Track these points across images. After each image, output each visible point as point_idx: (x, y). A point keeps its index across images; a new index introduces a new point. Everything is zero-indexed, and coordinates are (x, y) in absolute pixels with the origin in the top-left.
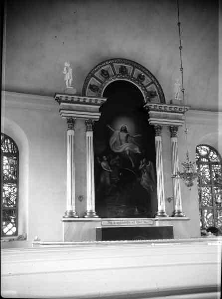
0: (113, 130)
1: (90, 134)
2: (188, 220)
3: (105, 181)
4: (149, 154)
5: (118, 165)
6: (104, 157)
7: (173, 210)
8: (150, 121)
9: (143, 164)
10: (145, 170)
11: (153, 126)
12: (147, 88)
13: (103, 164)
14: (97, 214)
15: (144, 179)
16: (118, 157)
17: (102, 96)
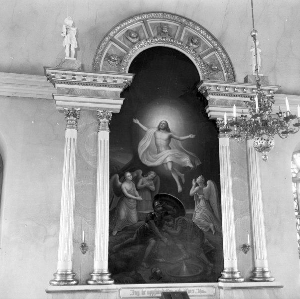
0: (144, 128)
1: (104, 136)
2: (281, 287)
3: (128, 216)
4: (208, 166)
5: (153, 188)
6: (128, 174)
7: (251, 268)
8: (209, 111)
9: (197, 185)
10: (200, 197)
11: (214, 121)
12: (204, 58)
13: (126, 187)
14: (111, 277)
15: (199, 213)
16: (152, 174)
17: (127, 72)
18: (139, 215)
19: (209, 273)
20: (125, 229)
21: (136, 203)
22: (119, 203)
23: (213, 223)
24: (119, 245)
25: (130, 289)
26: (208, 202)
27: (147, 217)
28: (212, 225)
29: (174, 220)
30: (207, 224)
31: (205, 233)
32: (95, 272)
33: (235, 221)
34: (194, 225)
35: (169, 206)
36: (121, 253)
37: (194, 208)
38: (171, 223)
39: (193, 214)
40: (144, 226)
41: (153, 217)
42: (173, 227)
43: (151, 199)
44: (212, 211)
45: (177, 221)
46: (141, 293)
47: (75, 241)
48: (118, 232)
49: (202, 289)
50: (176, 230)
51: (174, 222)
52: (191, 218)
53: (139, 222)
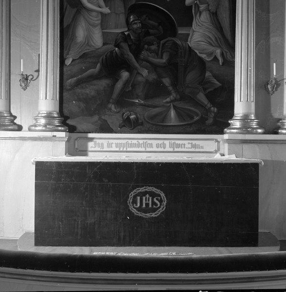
3: (88, 38)
15: (198, 36)
18: (104, 35)
19: (210, 121)
20: (84, 56)
21: (100, 17)
22: (75, 19)
23: (220, 47)
24: (76, 78)
26: (214, 15)
27: (116, 40)
28: (218, 52)
29: (160, 43)
30: (211, 49)
31: (208, 65)
35: (151, 22)
36: (78, 90)
37: (192, 26)
38: (153, 47)
40: (112, 52)
41: (126, 38)
42: (157, 54)
43: (123, 11)
44: (219, 28)
45: (164, 44)
46: (105, 145)
48: (73, 60)
49: (197, 142)
50: (162, 58)
51: (158, 46)
53: (106, 46)
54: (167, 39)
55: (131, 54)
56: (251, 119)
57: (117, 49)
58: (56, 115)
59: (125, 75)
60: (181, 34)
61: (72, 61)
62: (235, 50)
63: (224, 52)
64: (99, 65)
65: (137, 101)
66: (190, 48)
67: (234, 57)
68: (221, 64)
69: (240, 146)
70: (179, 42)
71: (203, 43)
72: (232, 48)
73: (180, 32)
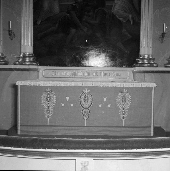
18: (61, 6)
24: (43, 33)
25: (52, 71)
28: (130, 16)
32: (21, 55)
33: (154, 12)
34: (113, 16)
38: (91, 14)
39: (112, 6)
41: (74, 8)
46: (62, 74)
47: (4, 30)
48: (41, 22)
49: (118, 72)
52: (111, 9)
54: (99, 9)
55: (77, 18)
56: (150, 58)
57: (68, 14)
58: (31, 55)
59: (73, 31)
60: (107, 5)
61: (41, 22)
62: (140, 15)
63: (134, 17)
64: (57, 24)
65: (81, 47)
66: (113, 14)
67: (140, 20)
68: (132, 24)
69: (143, 74)
70: (106, 10)
71: (121, 11)
72: (139, 14)
73: (107, 4)
